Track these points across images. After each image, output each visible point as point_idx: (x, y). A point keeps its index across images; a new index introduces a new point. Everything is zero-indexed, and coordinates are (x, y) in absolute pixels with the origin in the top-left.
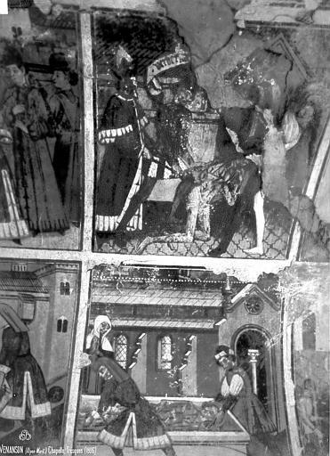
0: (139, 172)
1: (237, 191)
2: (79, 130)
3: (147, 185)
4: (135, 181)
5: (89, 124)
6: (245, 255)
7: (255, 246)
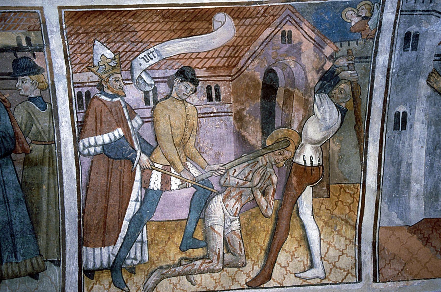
0: (137, 185)
1: (273, 194)
2: (52, 142)
3: (150, 199)
4: (133, 196)
5: (66, 133)
6: (299, 282)
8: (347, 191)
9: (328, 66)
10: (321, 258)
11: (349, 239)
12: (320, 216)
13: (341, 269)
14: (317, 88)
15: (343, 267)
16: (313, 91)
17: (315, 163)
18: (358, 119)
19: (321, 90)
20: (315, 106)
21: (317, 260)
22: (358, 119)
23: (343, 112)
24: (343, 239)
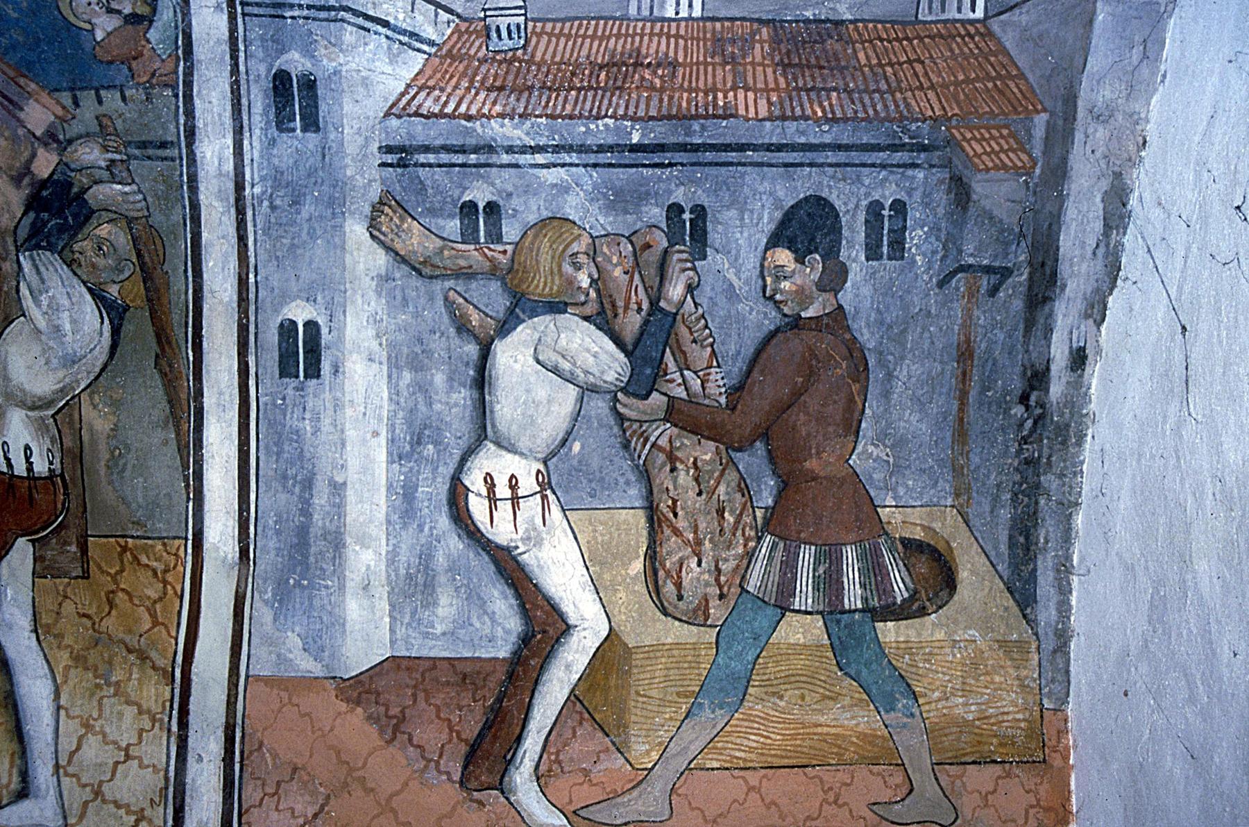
7: (23, 794)
8: (144, 560)
9: (45, 164)
10: (57, 766)
11: (149, 712)
12: (59, 636)
13: (118, 806)
14: (23, 233)
15: (125, 797)
16: (10, 240)
17: (41, 467)
18: (163, 337)
19: (37, 239)
20: (24, 290)
21: (43, 774)
22: (163, 337)
23: (115, 313)
24: (130, 712)
